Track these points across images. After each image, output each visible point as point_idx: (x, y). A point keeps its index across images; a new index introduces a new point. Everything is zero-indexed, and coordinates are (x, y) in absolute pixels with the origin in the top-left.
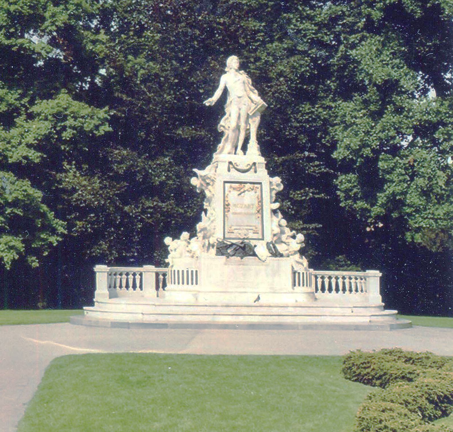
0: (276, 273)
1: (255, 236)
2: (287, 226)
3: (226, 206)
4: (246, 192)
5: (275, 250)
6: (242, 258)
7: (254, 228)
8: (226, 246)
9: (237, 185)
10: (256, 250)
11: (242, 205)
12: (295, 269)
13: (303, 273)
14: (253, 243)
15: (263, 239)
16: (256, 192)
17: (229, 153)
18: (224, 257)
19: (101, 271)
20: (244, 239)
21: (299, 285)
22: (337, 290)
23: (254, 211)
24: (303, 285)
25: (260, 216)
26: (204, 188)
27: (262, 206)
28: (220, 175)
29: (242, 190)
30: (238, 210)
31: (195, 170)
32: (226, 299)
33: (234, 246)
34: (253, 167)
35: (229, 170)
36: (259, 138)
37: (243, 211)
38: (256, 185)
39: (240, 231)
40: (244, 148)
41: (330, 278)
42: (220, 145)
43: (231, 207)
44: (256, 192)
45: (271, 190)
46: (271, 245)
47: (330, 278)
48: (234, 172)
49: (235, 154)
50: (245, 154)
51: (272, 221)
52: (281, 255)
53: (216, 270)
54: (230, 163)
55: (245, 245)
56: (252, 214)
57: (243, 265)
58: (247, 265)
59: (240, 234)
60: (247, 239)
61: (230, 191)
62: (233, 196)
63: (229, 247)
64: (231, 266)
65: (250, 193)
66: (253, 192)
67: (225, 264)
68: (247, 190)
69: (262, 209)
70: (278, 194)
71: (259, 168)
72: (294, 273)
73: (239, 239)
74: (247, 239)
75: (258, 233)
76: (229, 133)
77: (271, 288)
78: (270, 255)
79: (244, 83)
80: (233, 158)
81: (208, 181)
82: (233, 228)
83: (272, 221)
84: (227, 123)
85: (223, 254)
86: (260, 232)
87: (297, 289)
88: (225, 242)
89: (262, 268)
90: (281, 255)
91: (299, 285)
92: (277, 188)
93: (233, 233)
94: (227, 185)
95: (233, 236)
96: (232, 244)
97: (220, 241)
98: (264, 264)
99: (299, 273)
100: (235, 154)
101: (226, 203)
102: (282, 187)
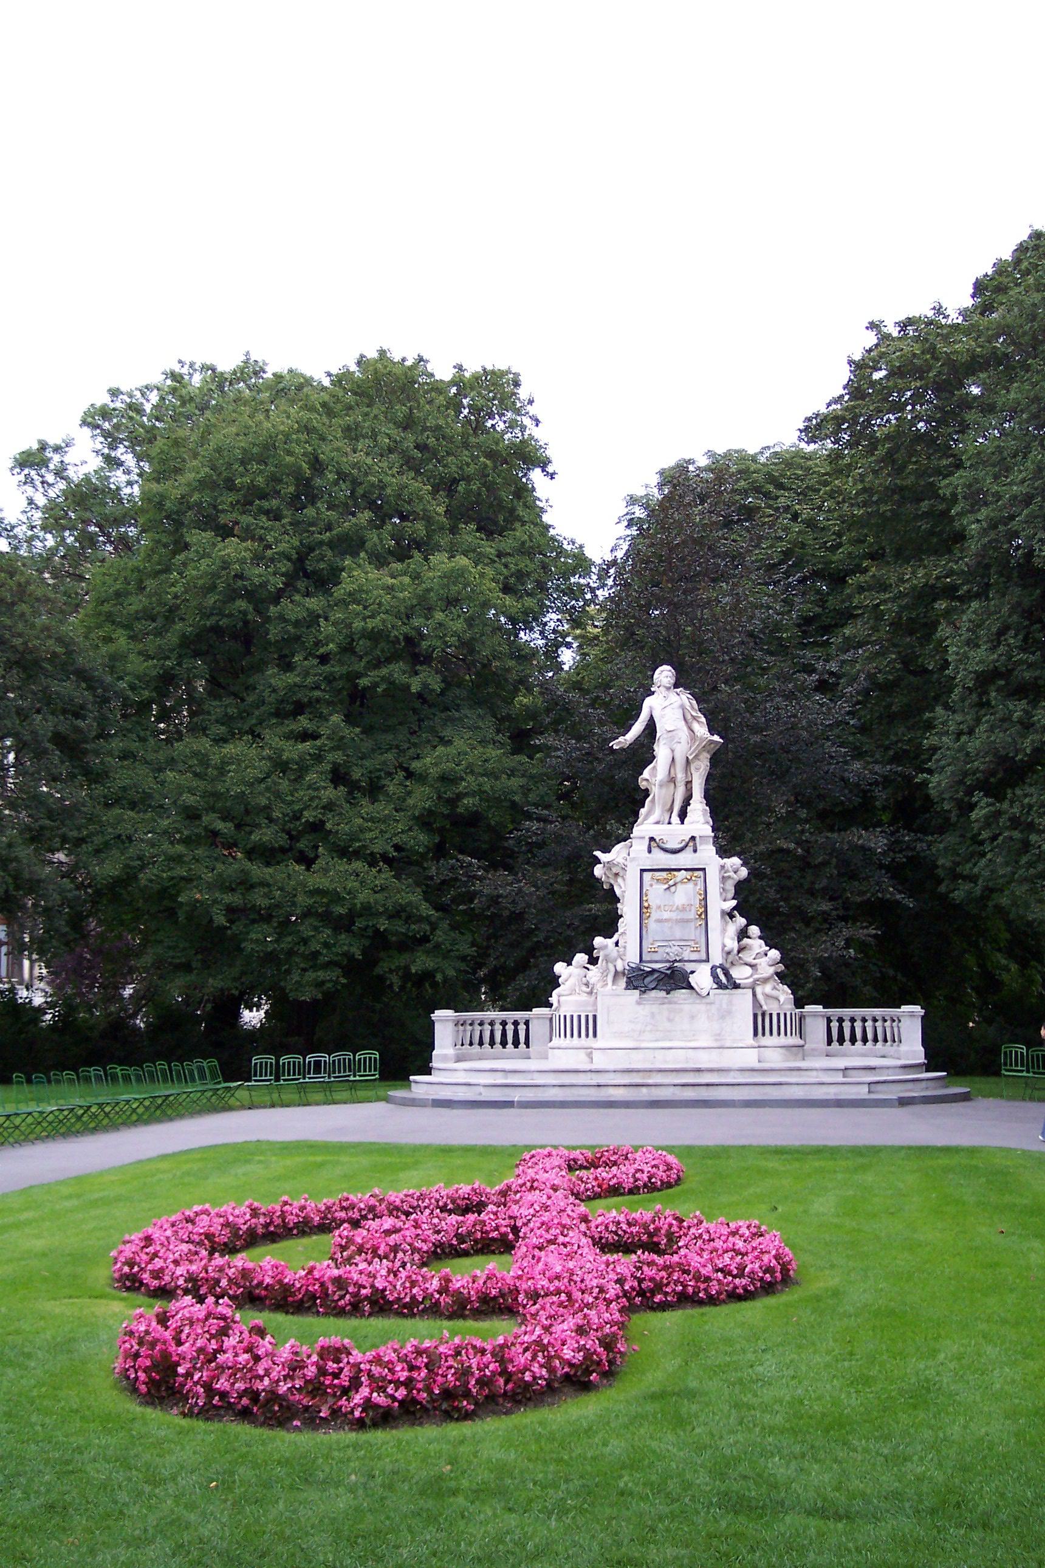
0: (725, 1014)
2: (760, 938)
3: (644, 909)
4: (679, 886)
6: (668, 993)
7: (692, 943)
9: (664, 874)
11: (672, 906)
12: (765, 1008)
13: (778, 1015)
14: (689, 967)
16: (696, 884)
17: (658, 823)
18: (637, 992)
19: (444, 1018)
20: (676, 961)
21: (771, 1034)
22: (865, 1040)
23: (692, 915)
24: (779, 1034)
25: (703, 922)
26: (612, 882)
27: (706, 907)
28: (633, 859)
29: (671, 883)
30: (666, 915)
31: (597, 853)
32: (638, 1061)
33: (656, 975)
34: (691, 844)
35: (650, 851)
36: (708, 797)
37: (674, 915)
38: (696, 873)
40: (683, 815)
41: (853, 1020)
42: (643, 811)
43: (653, 910)
44: (696, 884)
45: (724, 879)
46: (719, 970)
47: (853, 1020)
48: (658, 854)
49: (669, 823)
50: (682, 823)
51: (724, 931)
52: (736, 986)
53: (624, 1014)
54: (652, 839)
55: (673, 972)
56: (688, 921)
57: (670, 1003)
58: (676, 1003)
61: (651, 885)
62: (656, 893)
65: (684, 886)
66: (690, 885)
67: (639, 1003)
68: (681, 882)
69: (706, 911)
70: (740, 886)
71: (701, 844)
72: (763, 1015)
73: (669, 961)
74: (680, 961)
76: (655, 791)
77: (716, 1040)
78: (715, 986)
79: (683, 707)
80: (659, 831)
81: (614, 870)
83: (724, 931)
84: (653, 776)
85: (635, 988)
87: (767, 1040)
89: (702, 1007)
90: (736, 986)
91: (771, 1034)
92: (735, 876)
94: (647, 876)
95: (656, 957)
96: (654, 971)
97: (633, 965)
98: (704, 1001)
99: (771, 1015)
100: (669, 823)
101: (646, 904)
102: (744, 872)
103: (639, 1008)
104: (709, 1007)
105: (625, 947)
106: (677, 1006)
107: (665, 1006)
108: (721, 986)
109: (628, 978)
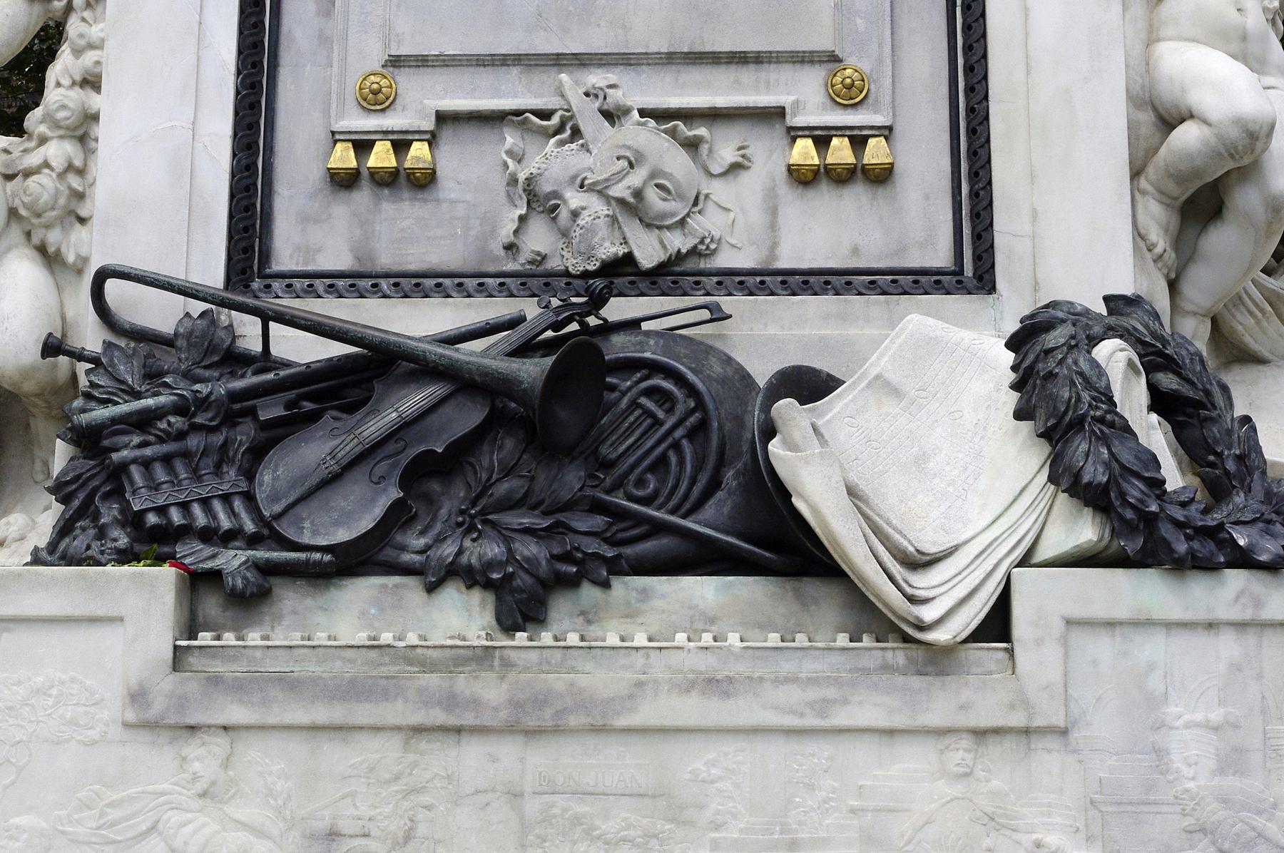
1: (823, 231)
5: (1194, 449)
6: (521, 607)
7: (806, 97)
8: (235, 409)
10: (815, 464)
15: (973, 271)
18: (150, 592)
20: (621, 273)
39: (552, 162)
46: (1113, 355)
57: (530, 724)
59: (539, 201)
60: (669, 275)
63: (295, 423)
64: (268, 766)
73: (536, 279)
74: (669, 275)
75: (881, 177)
78: (1084, 531)
82: (419, 101)
86: (924, 158)
88: (248, 331)
93: (424, 181)
97: (160, 313)
98: (942, 703)
103: (160, 770)
104: (999, 773)
105: (83, 130)
106: (616, 764)
107: (472, 761)
108: (1139, 533)
109: (89, 441)
